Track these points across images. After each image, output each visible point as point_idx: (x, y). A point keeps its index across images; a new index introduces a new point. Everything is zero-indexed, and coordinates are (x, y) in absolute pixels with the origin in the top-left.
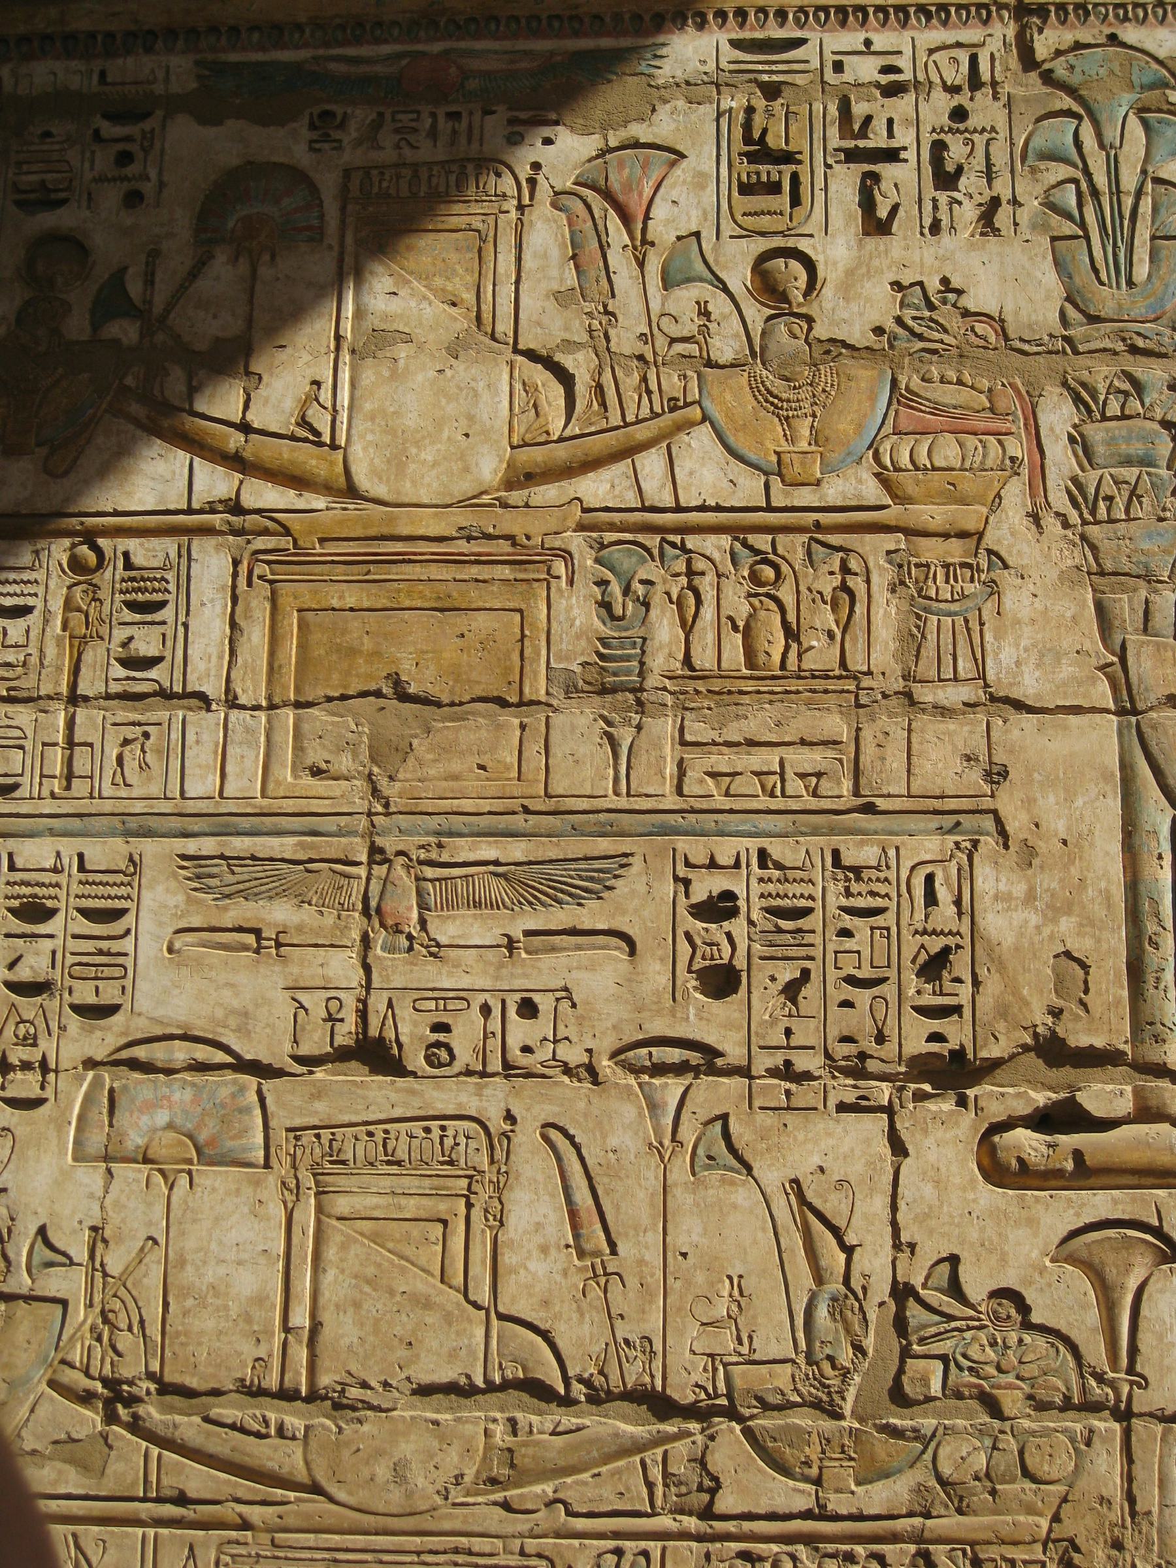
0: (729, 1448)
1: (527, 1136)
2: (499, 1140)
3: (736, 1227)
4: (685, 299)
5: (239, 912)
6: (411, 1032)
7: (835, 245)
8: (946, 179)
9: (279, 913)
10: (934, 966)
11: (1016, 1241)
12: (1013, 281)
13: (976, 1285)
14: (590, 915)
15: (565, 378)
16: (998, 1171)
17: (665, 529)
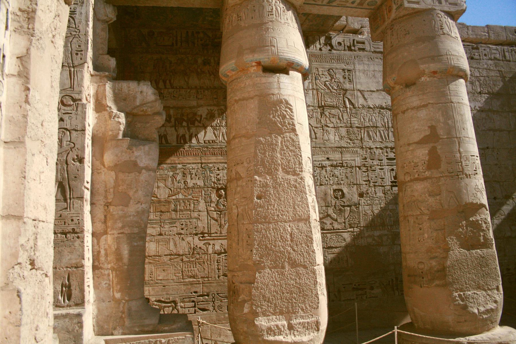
0: (184, 257)
1: (171, 239)
2: (169, 239)
3: (184, 244)
4: (179, 184)
5: (152, 226)
6: (163, 233)
7: (189, 181)
8: (196, 176)
9: (154, 226)
10: (195, 228)
11: (201, 244)
12: (200, 183)
13: (198, 247)
14: (174, 225)
15: (171, 190)
16: (200, 240)
17: (178, 200)
